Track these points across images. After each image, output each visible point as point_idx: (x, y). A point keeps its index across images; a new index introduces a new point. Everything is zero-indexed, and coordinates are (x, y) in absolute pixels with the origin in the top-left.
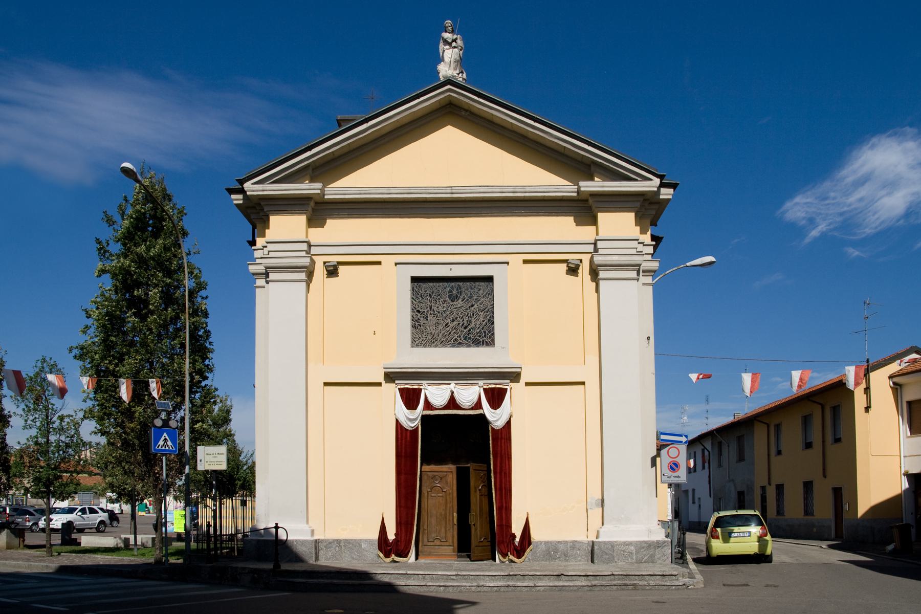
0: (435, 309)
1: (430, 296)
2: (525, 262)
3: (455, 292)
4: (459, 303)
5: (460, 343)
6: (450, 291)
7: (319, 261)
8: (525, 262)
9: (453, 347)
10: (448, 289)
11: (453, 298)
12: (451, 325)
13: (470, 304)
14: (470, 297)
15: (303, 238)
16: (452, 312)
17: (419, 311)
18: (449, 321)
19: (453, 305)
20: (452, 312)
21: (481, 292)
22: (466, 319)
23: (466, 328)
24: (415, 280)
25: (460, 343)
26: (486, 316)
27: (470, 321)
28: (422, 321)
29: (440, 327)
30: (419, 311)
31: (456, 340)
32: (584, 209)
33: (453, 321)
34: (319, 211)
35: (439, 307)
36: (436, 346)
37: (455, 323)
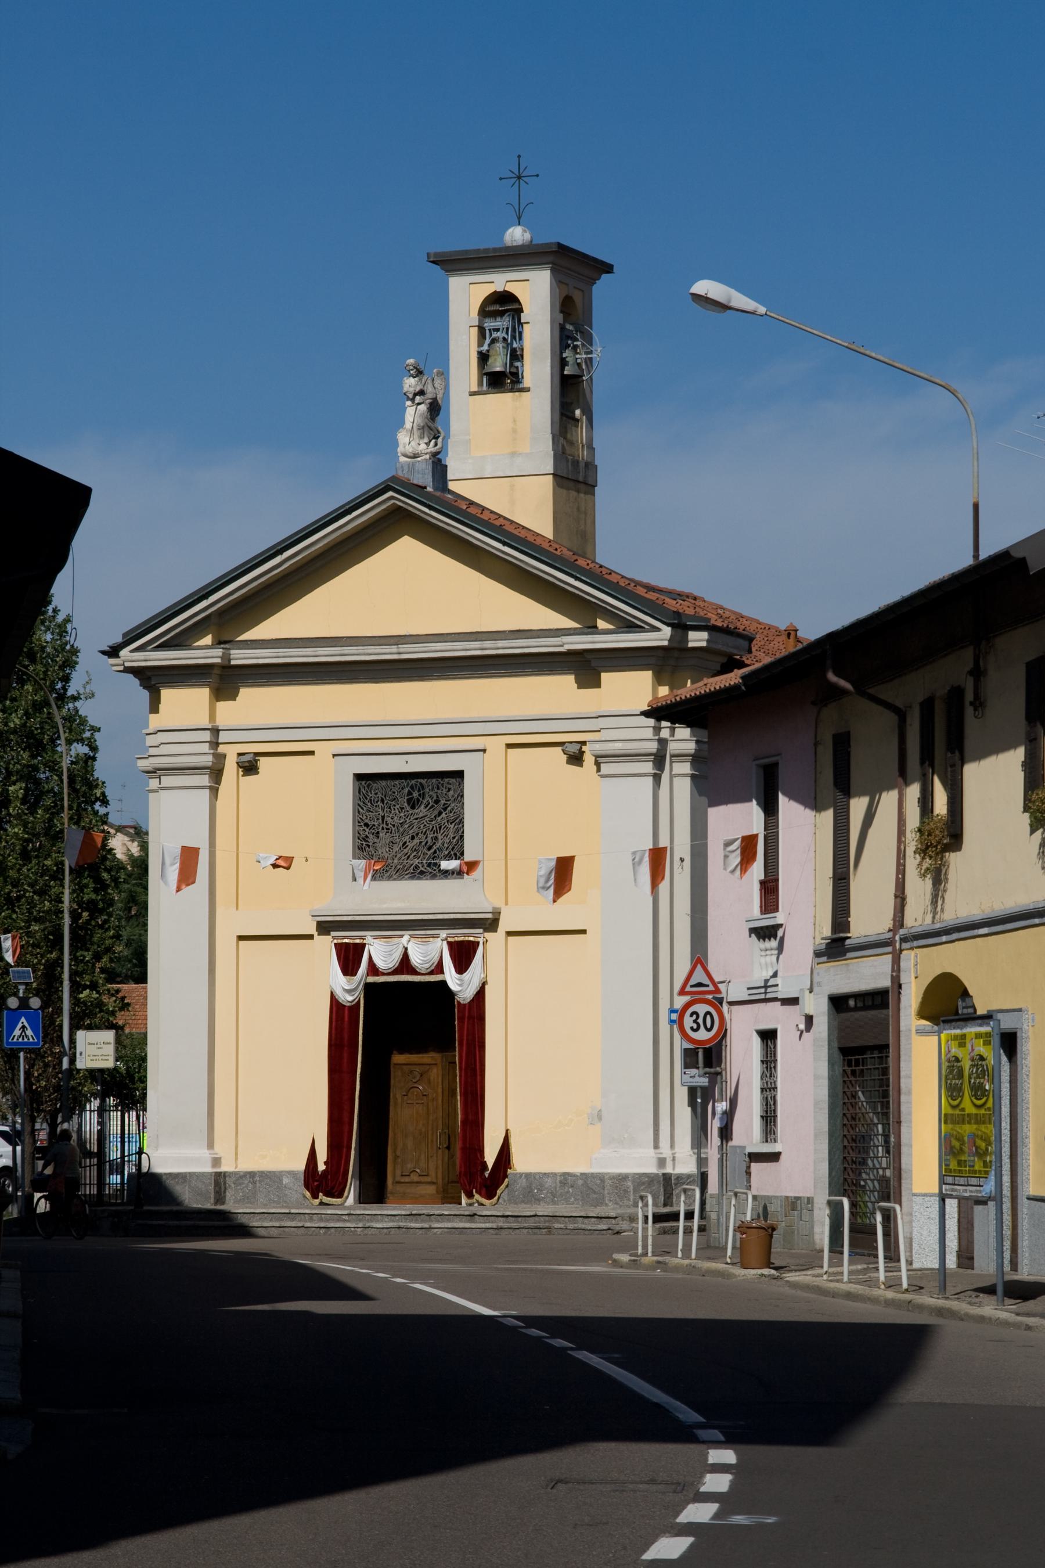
0: (389, 820)
1: (383, 801)
2: (509, 746)
3: (415, 794)
4: (421, 811)
5: (422, 873)
6: (410, 793)
7: (231, 754)
8: (509, 746)
9: (412, 878)
10: (406, 790)
11: (413, 804)
12: (410, 845)
13: (436, 812)
14: (437, 802)
15: (205, 723)
16: (411, 826)
17: (366, 825)
18: (407, 838)
19: (410, 815)
20: (411, 826)
21: (451, 793)
22: (430, 835)
23: (429, 849)
24: (359, 777)
25: (422, 873)
26: (457, 830)
27: (436, 838)
28: (372, 839)
29: (396, 848)
30: (366, 825)
31: (417, 867)
32: (586, 667)
33: (413, 838)
34: (225, 681)
35: (395, 818)
36: (390, 878)
37: (416, 841)
